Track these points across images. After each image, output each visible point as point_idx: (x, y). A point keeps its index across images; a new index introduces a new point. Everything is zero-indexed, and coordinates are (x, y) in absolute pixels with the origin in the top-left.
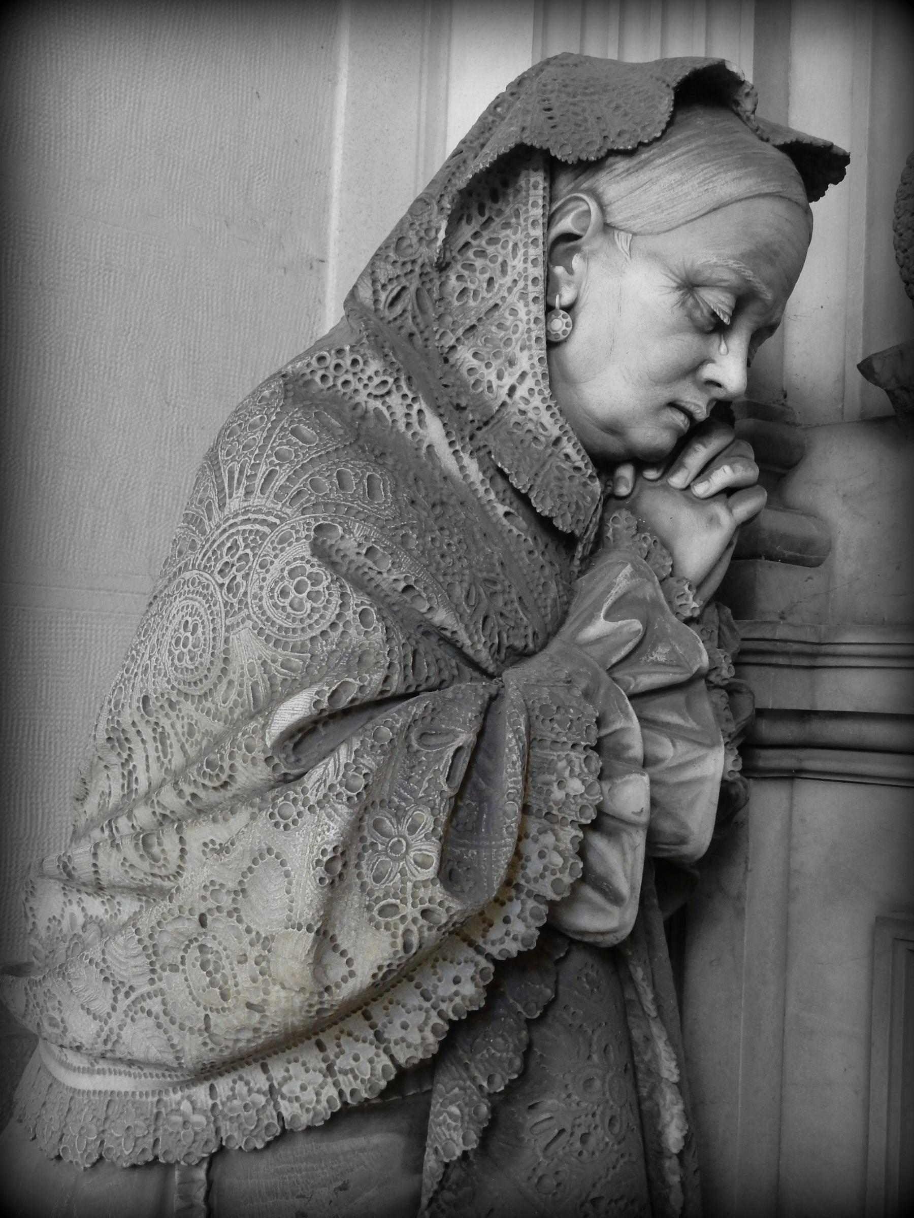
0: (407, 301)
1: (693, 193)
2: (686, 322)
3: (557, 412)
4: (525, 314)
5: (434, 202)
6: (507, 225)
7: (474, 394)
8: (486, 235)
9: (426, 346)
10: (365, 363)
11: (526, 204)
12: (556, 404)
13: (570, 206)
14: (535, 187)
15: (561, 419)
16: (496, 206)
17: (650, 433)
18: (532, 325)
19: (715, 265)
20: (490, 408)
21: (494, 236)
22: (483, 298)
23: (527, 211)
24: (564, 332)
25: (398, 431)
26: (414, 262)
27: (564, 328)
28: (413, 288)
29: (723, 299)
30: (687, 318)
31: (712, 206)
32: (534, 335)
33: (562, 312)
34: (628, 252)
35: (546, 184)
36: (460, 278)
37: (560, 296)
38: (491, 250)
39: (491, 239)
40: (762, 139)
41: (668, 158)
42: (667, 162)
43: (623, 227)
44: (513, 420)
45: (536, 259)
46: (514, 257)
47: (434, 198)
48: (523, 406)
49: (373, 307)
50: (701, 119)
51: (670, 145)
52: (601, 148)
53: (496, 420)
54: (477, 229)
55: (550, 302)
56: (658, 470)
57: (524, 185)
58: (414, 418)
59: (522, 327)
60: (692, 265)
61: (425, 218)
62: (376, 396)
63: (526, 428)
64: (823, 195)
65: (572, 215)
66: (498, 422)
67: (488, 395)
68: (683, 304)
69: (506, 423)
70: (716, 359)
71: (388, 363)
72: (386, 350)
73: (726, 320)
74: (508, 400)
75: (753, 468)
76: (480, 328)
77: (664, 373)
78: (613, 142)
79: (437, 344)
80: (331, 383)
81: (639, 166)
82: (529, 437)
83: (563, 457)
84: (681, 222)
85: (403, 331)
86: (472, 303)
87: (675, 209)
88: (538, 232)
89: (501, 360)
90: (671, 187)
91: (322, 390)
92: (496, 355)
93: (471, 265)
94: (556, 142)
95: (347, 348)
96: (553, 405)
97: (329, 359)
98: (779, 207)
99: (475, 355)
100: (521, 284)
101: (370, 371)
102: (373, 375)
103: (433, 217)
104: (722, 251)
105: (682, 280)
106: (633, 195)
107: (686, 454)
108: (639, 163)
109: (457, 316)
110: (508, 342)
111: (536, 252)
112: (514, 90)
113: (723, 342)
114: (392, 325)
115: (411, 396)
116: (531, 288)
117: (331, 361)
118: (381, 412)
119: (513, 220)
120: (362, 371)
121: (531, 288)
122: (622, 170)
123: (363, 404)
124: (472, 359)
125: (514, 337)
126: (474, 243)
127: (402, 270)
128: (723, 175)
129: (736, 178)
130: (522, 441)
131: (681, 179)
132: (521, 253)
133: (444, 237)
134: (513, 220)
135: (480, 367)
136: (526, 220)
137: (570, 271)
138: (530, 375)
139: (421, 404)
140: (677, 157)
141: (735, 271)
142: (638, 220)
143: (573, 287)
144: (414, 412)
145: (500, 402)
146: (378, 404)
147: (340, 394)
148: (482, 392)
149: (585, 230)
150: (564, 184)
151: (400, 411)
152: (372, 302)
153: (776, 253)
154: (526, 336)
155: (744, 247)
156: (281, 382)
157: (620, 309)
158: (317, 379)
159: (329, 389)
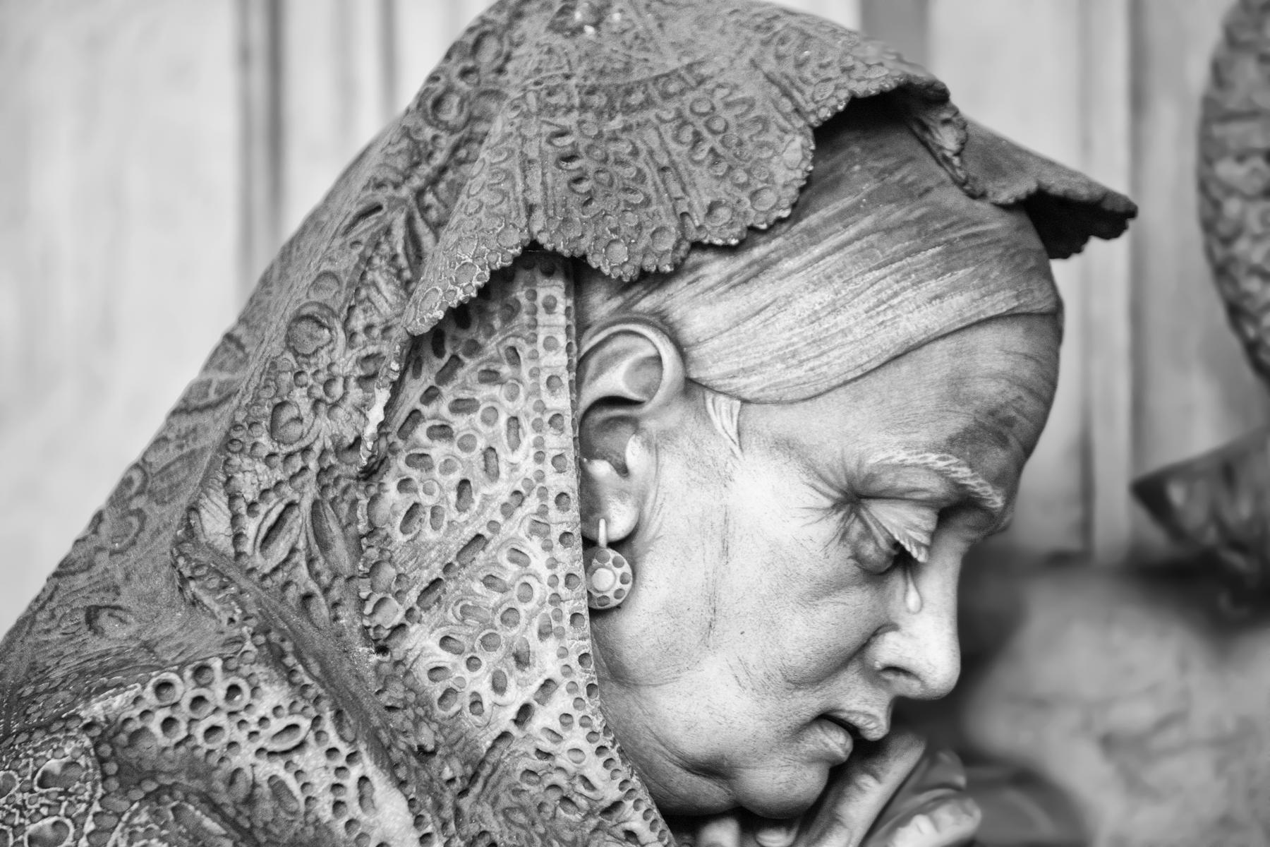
0: (295, 531)
1: (857, 330)
2: (850, 568)
3: (616, 756)
4: (546, 565)
5: (338, 325)
6: (490, 377)
7: (444, 719)
8: (449, 393)
9: (336, 618)
10: (255, 690)
11: (532, 340)
12: (614, 742)
13: (619, 344)
14: (550, 308)
15: (624, 769)
16: (465, 336)
17: (784, 776)
18: (562, 590)
19: (902, 465)
20: (473, 744)
21: (465, 395)
22: (450, 523)
23: (534, 356)
24: (618, 593)
25: (317, 820)
26: (306, 450)
27: (619, 585)
28: (306, 504)
29: (916, 520)
30: (852, 562)
31: (892, 352)
32: (567, 609)
33: (612, 554)
34: (735, 437)
35: (570, 302)
36: (404, 485)
37: (608, 522)
38: (460, 424)
39: (458, 401)
40: (972, 196)
41: (806, 257)
42: (805, 266)
43: (723, 389)
44: (521, 766)
45: (561, 456)
46: (515, 446)
47: (337, 316)
48: (547, 746)
49: (232, 551)
50: (861, 169)
51: (811, 232)
52: (679, 243)
53: (487, 770)
54: (431, 381)
55: (592, 534)
56: (788, 834)
57: (524, 301)
58: (351, 794)
59: (541, 590)
60: (860, 465)
61: (323, 359)
62: (272, 753)
63: (548, 782)
64: (1078, 250)
65: (625, 365)
66: (494, 770)
67: (470, 720)
68: (844, 535)
69: (508, 773)
70: (900, 622)
71: (297, 689)
72: (290, 660)
73: (920, 556)
74: (514, 730)
75: (970, 814)
76: (451, 585)
77: (813, 665)
78: (700, 228)
79: (367, 623)
80: (183, 734)
81: (749, 272)
82: (554, 796)
83: (622, 835)
84: (834, 382)
85: (292, 593)
86: (429, 535)
87: (825, 359)
88: (561, 402)
89: (498, 654)
90: (815, 318)
91: (165, 749)
92: (489, 643)
93: (424, 455)
94: (597, 238)
95: (217, 664)
96: (609, 744)
97: (179, 688)
98: (1014, 337)
99: (445, 641)
100: (532, 504)
101: (264, 708)
102: (270, 715)
103: (336, 355)
104: (914, 436)
105: (841, 491)
106: (742, 329)
107: (840, 796)
108: (750, 265)
109: (404, 563)
110: (510, 617)
111: (561, 442)
112: (470, 64)
113: (911, 586)
114: (268, 582)
115: (345, 750)
116: (554, 514)
117: (184, 690)
118: (282, 784)
119: (506, 370)
120: (248, 707)
121: (554, 514)
122: (716, 278)
123: (248, 771)
124: (438, 650)
125: (523, 608)
126: (426, 410)
127: (285, 470)
128: (909, 294)
129: (936, 297)
130: (541, 806)
131: (834, 302)
132: (529, 437)
133: (382, 418)
134: (506, 370)
135: (454, 665)
136: (534, 374)
137: (623, 470)
138: (563, 688)
139: (367, 765)
140: (822, 257)
141: (940, 473)
142: (754, 379)
143: (629, 502)
144: (351, 781)
145: (497, 733)
146: (277, 768)
147: (200, 753)
148: (459, 712)
149: (650, 391)
150: (602, 305)
151: (321, 780)
152: (230, 541)
153: (1009, 422)
154: (549, 609)
155: (956, 423)
156: (87, 743)
157: (726, 550)
158: (155, 726)
159: (178, 744)
